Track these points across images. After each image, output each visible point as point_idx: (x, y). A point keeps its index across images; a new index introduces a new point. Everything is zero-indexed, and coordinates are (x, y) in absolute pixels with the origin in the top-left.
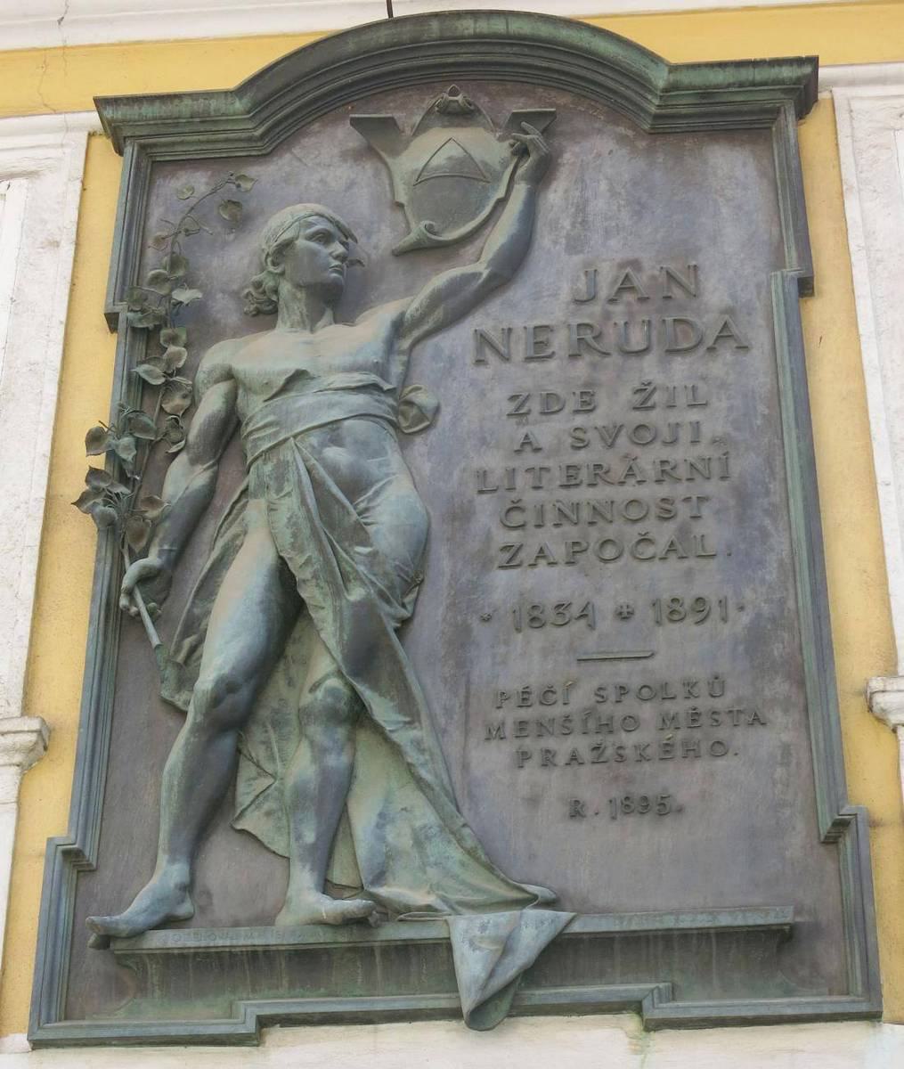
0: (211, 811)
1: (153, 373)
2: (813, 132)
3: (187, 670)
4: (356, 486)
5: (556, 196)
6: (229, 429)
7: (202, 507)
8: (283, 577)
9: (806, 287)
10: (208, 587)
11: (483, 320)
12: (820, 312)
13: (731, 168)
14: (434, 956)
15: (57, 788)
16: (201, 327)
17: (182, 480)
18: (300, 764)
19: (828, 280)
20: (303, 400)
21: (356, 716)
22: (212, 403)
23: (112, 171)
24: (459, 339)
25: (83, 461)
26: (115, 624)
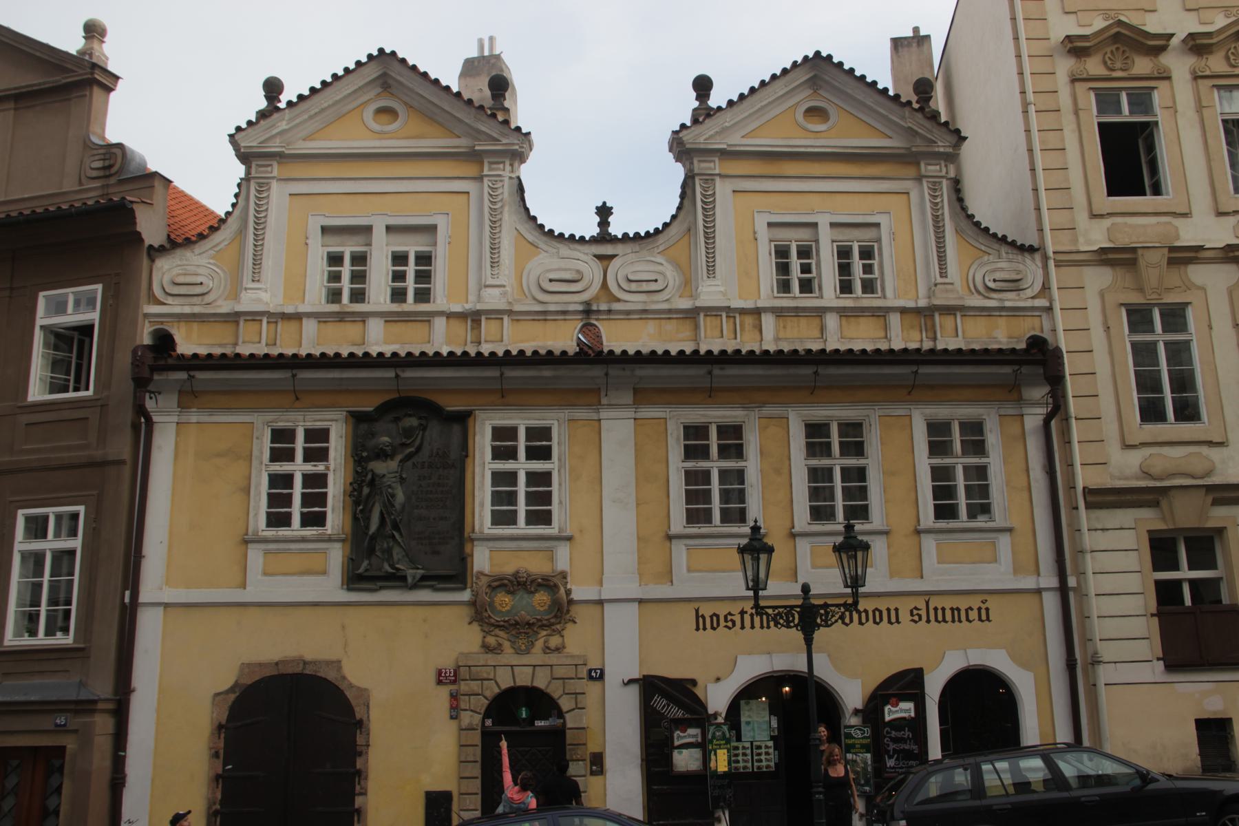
0: (371, 552)
1: (359, 469)
2: (471, 420)
3: (367, 527)
4: (393, 496)
5: (427, 433)
6: (373, 480)
7: (369, 495)
8: (382, 514)
9: (467, 456)
10: (371, 511)
11: (414, 460)
12: (469, 461)
13: (456, 428)
14: (404, 578)
15: (348, 545)
16: (368, 459)
17: (366, 490)
18: (385, 545)
19: (471, 453)
20: (385, 480)
21: (393, 537)
22: (369, 476)
23: (351, 420)
24: (409, 463)
25: (350, 489)
26: (355, 519)
